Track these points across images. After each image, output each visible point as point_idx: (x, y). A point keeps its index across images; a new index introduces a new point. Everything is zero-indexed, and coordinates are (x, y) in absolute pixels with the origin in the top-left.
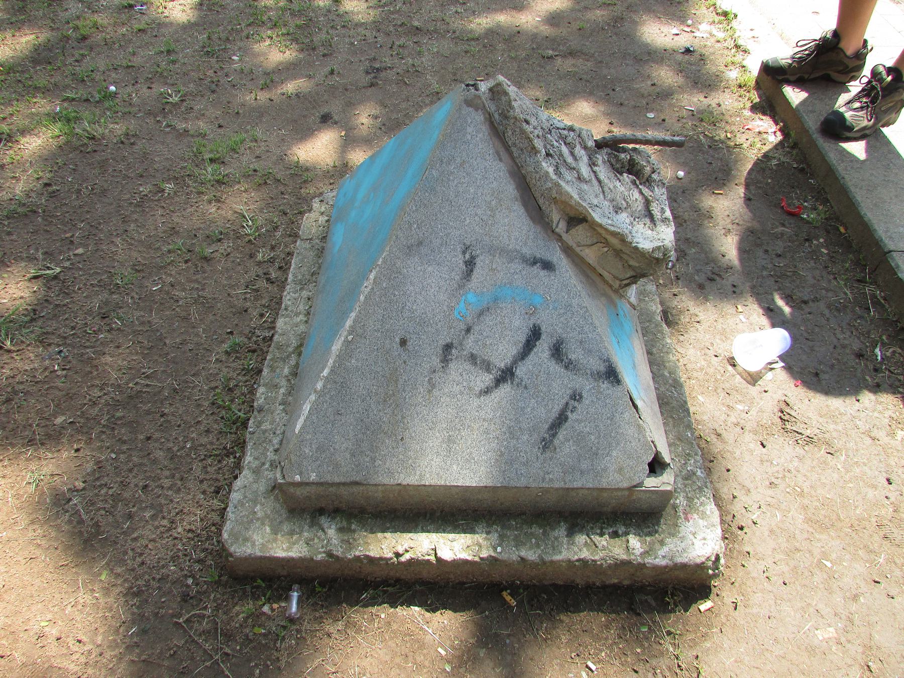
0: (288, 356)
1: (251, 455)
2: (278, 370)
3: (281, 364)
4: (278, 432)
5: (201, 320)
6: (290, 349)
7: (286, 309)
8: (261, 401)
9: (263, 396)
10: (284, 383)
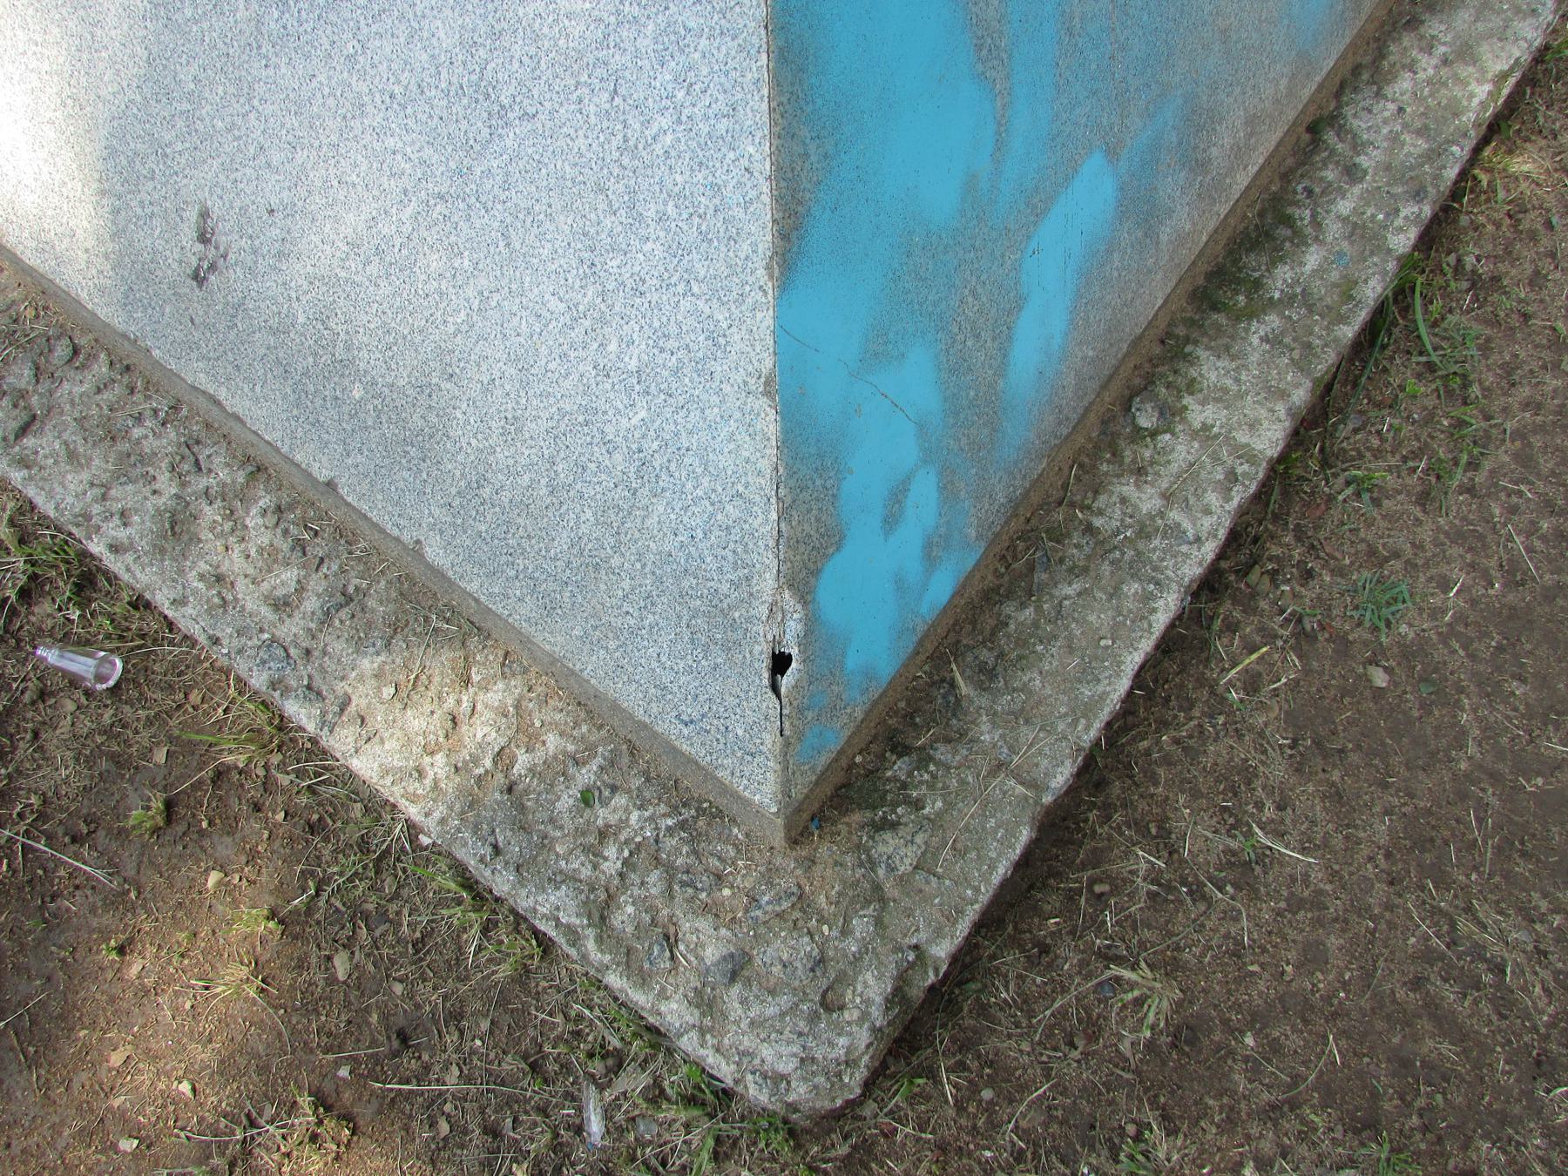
0: (1288, 300)
1: (1472, 96)
2: (1334, 276)
3: (1319, 289)
4: (1392, 107)
5: (1463, 796)
6: (1273, 321)
7: (1232, 477)
8: (1408, 210)
9: (1399, 222)
10: (1333, 229)
